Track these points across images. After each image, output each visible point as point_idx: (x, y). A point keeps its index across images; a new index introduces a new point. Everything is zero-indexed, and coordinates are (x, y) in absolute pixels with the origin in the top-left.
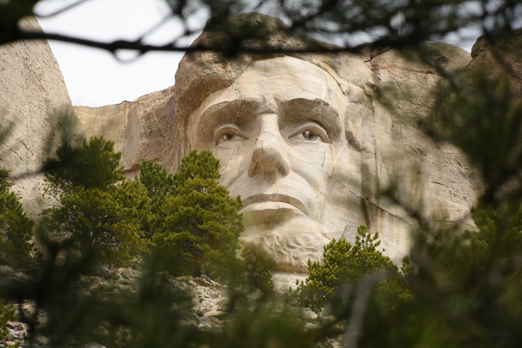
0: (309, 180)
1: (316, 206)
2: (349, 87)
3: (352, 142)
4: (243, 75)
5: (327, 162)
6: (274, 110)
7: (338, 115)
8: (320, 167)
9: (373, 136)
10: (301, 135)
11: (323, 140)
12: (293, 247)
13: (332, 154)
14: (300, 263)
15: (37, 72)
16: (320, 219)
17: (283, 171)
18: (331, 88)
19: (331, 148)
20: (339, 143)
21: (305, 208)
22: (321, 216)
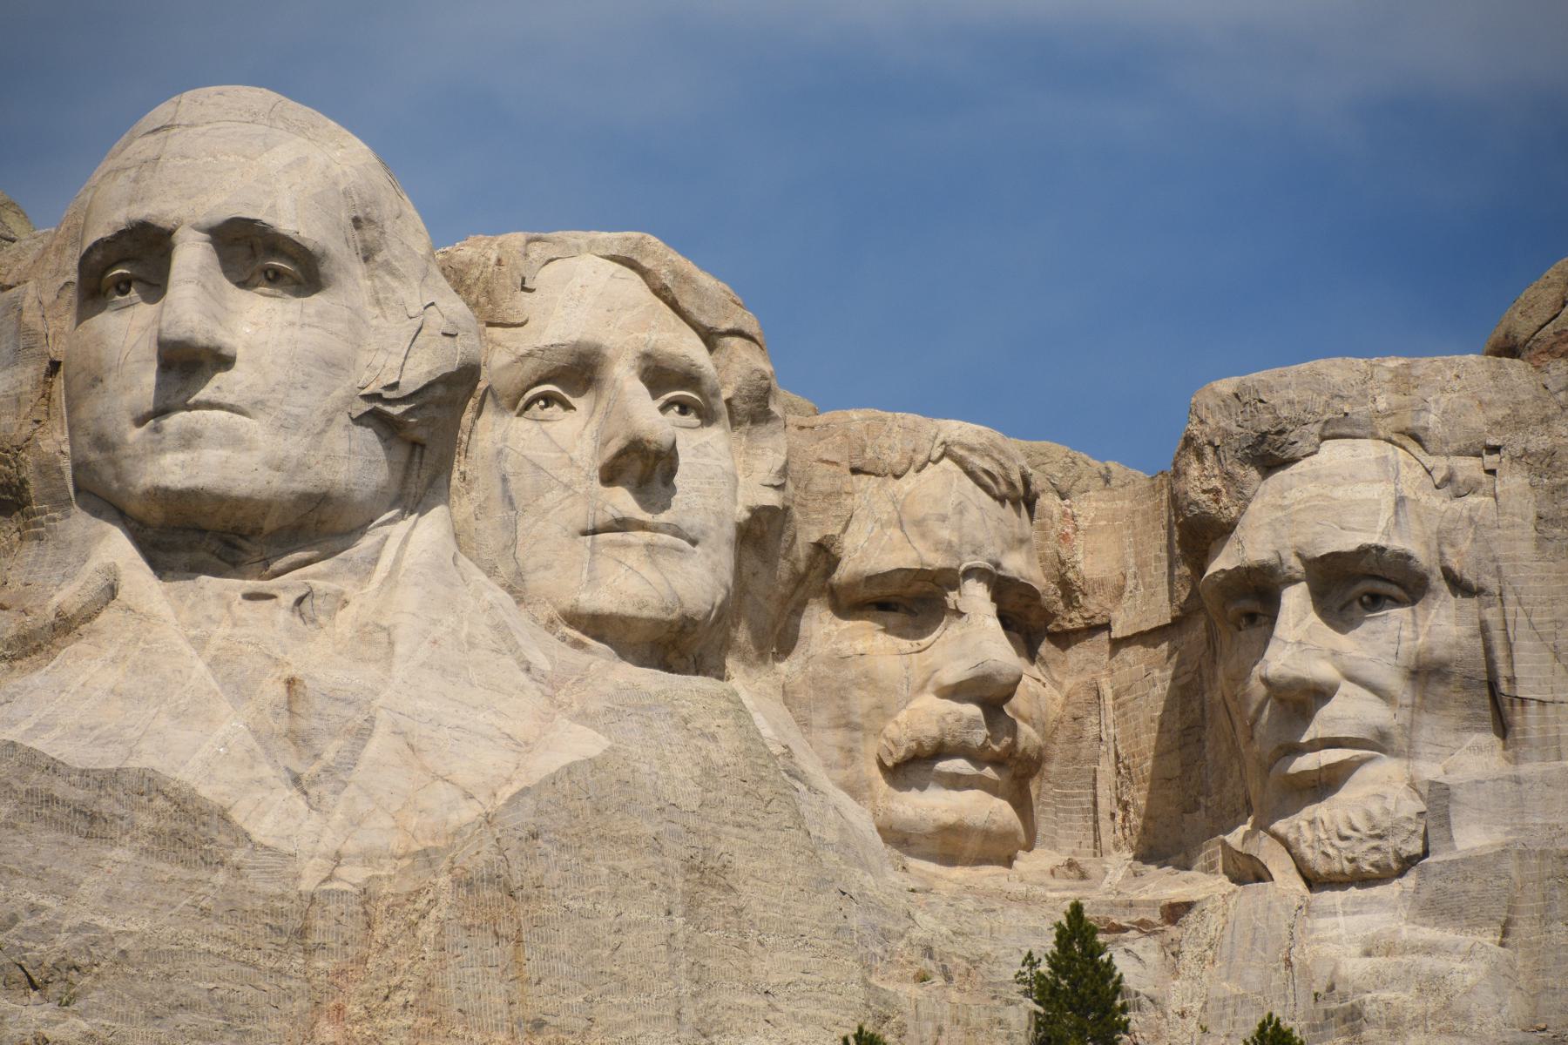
0: (1376, 690)
1: (1396, 732)
2: (1449, 468)
3: (1458, 586)
4: (1251, 507)
5: (1404, 645)
6: (1298, 576)
7: (1409, 558)
8: (1392, 660)
9: (1494, 560)
10: (1357, 605)
11: (1398, 603)
12: (1346, 838)
13: (1415, 624)
14: (1358, 868)
15: (718, 865)
16: (1409, 753)
17: (1321, 693)
18: (1406, 493)
19: (1414, 612)
20: (1431, 596)
21: (1379, 742)
22: (1410, 747)
